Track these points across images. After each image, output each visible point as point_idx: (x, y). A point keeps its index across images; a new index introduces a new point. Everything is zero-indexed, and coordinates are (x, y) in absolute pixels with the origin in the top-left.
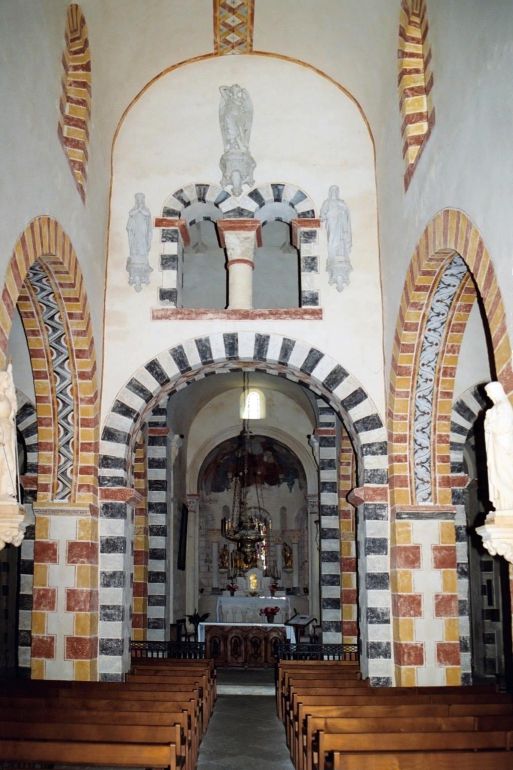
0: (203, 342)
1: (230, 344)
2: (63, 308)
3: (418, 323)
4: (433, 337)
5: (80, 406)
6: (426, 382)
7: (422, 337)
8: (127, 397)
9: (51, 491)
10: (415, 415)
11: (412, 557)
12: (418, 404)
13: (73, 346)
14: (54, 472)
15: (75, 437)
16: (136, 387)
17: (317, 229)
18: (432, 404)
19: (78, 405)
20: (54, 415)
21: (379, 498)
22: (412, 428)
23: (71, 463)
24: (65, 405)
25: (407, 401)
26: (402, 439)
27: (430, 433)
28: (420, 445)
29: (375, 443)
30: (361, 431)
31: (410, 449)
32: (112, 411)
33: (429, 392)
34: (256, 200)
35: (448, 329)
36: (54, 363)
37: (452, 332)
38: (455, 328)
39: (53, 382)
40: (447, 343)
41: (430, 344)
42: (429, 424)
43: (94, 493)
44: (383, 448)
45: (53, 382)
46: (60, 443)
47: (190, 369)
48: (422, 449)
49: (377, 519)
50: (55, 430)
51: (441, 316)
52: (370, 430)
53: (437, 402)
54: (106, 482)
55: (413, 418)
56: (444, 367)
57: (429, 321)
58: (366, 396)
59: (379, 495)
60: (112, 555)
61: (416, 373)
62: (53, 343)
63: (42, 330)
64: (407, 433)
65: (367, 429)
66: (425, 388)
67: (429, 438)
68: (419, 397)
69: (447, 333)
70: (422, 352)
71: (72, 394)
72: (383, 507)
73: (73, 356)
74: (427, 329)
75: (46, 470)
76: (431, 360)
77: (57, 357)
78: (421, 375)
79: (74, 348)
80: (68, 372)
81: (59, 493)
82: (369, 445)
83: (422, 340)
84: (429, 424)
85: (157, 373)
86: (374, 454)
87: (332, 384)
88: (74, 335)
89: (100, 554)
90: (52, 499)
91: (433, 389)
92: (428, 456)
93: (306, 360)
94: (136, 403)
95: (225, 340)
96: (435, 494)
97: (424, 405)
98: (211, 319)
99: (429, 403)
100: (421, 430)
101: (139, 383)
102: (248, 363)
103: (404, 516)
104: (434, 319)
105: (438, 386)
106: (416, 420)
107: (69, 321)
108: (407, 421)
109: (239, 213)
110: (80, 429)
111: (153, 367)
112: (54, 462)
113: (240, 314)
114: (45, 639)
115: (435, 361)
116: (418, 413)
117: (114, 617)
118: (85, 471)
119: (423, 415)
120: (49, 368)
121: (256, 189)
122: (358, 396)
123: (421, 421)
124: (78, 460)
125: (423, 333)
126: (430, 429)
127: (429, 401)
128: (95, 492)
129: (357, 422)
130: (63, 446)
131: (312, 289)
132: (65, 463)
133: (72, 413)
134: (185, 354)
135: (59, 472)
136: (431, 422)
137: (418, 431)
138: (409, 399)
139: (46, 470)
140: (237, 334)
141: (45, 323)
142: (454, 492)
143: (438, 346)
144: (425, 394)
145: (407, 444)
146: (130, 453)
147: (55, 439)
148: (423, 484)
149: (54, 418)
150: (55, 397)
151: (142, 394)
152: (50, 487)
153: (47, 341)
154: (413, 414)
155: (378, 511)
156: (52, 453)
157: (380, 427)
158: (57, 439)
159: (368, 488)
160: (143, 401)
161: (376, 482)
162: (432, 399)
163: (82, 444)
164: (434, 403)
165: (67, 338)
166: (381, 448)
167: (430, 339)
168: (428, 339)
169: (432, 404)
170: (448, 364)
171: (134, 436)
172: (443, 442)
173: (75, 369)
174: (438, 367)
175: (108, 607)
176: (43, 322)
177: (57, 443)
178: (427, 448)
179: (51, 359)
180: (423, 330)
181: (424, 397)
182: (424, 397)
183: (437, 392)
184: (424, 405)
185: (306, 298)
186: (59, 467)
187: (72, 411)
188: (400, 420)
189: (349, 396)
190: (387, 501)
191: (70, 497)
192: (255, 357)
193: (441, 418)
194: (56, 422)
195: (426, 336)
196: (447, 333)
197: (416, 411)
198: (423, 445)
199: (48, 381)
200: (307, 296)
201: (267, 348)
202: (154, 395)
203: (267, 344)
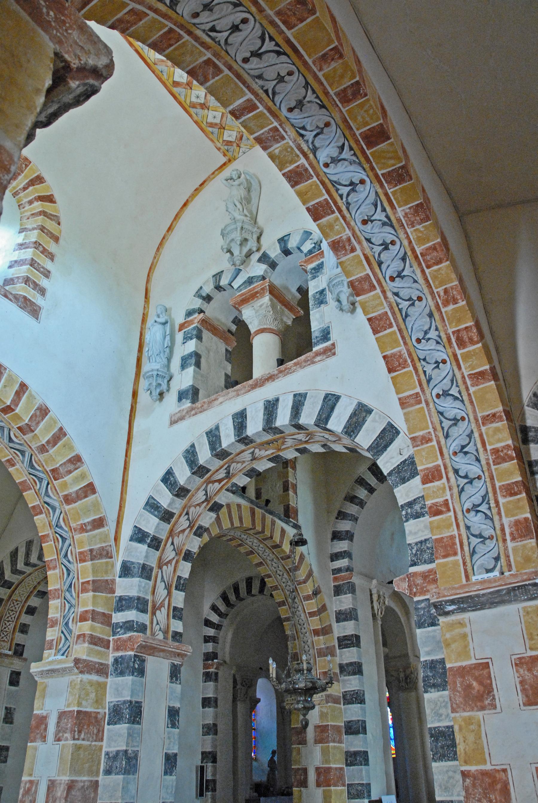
10: (443, 428)
12: (441, 409)
18: (462, 401)
22: (445, 450)
27: (477, 450)
28: (466, 477)
33: (450, 383)
48: (471, 482)
53: (469, 395)
64: (440, 462)
68: (438, 396)
92: (483, 492)
99: (457, 402)
100: (460, 452)
106: (447, 436)
108: (434, 443)
116: (446, 424)
119: (455, 424)
123: (456, 435)
127: (456, 398)
136: (472, 432)
137: (455, 453)
138: (423, 405)
144: (446, 388)
145: (444, 480)
162: (460, 392)
164: (466, 398)
169: (462, 401)
173: (58, 494)
178: (479, 478)
181: (446, 394)
182: (446, 394)
183: (463, 377)
188: (422, 444)
197: (441, 422)
198: (471, 476)
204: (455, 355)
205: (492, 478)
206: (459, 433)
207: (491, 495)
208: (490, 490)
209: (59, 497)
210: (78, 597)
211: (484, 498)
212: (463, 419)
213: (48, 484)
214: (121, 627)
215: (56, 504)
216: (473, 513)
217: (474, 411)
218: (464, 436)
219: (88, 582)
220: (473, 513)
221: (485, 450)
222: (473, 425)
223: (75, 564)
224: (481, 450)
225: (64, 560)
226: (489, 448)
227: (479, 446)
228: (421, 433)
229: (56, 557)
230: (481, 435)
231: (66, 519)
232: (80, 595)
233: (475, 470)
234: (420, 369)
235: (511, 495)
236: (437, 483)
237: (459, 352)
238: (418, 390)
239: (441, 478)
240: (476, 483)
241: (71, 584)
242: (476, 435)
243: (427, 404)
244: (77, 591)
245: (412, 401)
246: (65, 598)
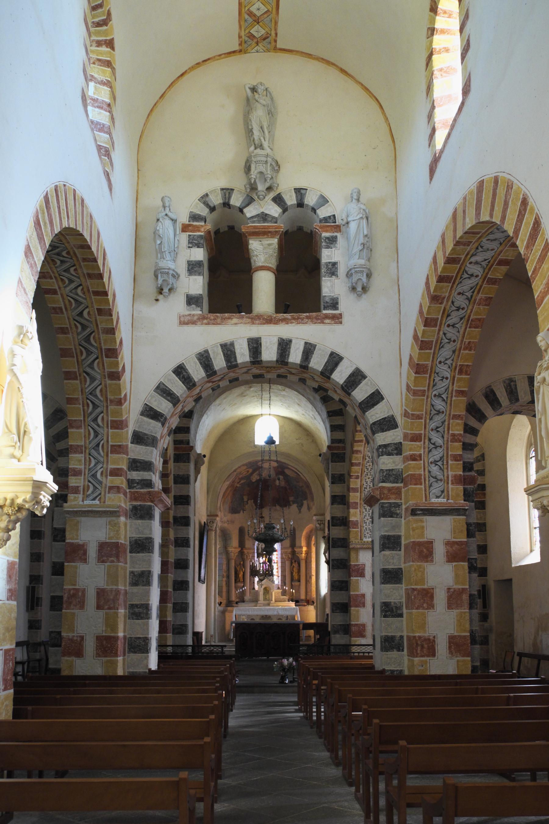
0: (228, 346)
1: (253, 348)
2: (92, 303)
3: (438, 318)
4: (451, 333)
5: (109, 407)
6: (442, 380)
7: (441, 333)
8: (155, 401)
9: (82, 492)
10: (430, 414)
11: (424, 551)
12: (433, 403)
13: (102, 344)
14: (85, 474)
15: (105, 439)
16: (163, 391)
17: (338, 235)
18: (446, 403)
19: (107, 407)
20: (84, 417)
21: (394, 496)
23: (101, 465)
24: (95, 406)
25: (424, 399)
26: (416, 438)
27: (444, 431)
28: (434, 444)
29: (391, 444)
30: (378, 433)
31: (424, 448)
32: (141, 415)
33: (444, 391)
34: (279, 205)
35: (467, 324)
36: (83, 363)
37: (470, 328)
38: (473, 323)
39: (83, 382)
40: (464, 340)
41: (447, 341)
42: (443, 423)
43: (124, 494)
44: (397, 449)
45: (83, 382)
46: (90, 446)
47: (215, 373)
48: (436, 448)
49: (391, 517)
50: (85, 432)
51: (461, 310)
52: (386, 431)
53: (451, 401)
54: (136, 485)
55: (428, 417)
56: (460, 365)
57: (448, 315)
58: (383, 398)
59: (394, 493)
60: (141, 554)
61: (433, 371)
62: (83, 342)
63: (71, 328)
64: (423, 432)
65: (383, 430)
66: (442, 386)
67: (443, 437)
68: (435, 396)
69: (466, 328)
70: (439, 349)
71: (102, 395)
72: (398, 506)
73: (102, 354)
74: (446, 324)
75: (77, 473)
76: (448, 357)
77: (87, 357)
78: (437, 373)
79: (103, 347)
80: (97, 372)
81: (89, 495)
82: (385, 446)
83: (441, 336)
84: (443, 423)
85: (183, 377)
86: (389, 454)
87: (351, 387)
88: (103, 333)
89: (129, 554)
90: (83, 501)
91: (448, 387)
92: (441, 455)
93: (326, 363)
94: (163, 406)
95: (249, 345)
96: (448, 491)
97: (439, 404)
98: (236, 324)
99: (444, 402)
100: (435, 429)
101: (167, 387)
102: (271, 367)
103: (419, 512)
104: (454, 314)
105: (453, 384)
106: (431, 419)
107: (98, 317)
108: (423, 421)
109: (263, 218)
110: (110, 431)
111: (180, 371)
112: (85, 464)
113: (263, 319)
114: (75, 638)
115: (452, 358)
117: (142, 615)
118: (116, 473)
119: (438, 414)
120: (79, 368)
121: (279, 194)
122: (376, 398)
123: (436, 420)
124: (108, 462)
125: (442, 329)
126: (444, 428)
127: (444, 400)
128: (125, 494)
129: (374, 424)
130: (93, 448)
131: (332, 295)
132: (95, 465)
133: (102, 415)
134: (211, 359)
135: (89, 475)
136: (445, 421)
137: (432, 430)
138: (425, 398)
139: (77, 473)
140: (261, 338)
141: (74, 320)
142: (465, 490)
143: (456, 343)
144: (441, 393)
146: (158, 458)
147: (85, 442)
148: (436, 482)
149: (84, 420)
150: (85, 399)
151: (169, 398)
152: (81, 489)
153: (77, 340)
154: (428, 413)
155: (393, 509)
156: (83, 455)
157: (395, 428)
158: (87, 442)
159: (384, 487)
160: (170, 405)
161: (390, 482)
162: (447, 398)
163: (112, 446)
164: (449, 402)
165: (97, 336)
166: (396, 449)
167: (449, 335)
168: (447, 335)
169: (446, 403)
170: (463, 362)
171: (162, 441)
172: (456, 441)
173: (104, 369)
174: (454, 365)
175: (137, 606)
176: (72, 319)
177: (87, 446)
178: (441, 447)
179: (80, 359)
180: (442, 326)
181: (440, 396)
182: (440, 396)
183: (452, 390)
184: (439, 404)
185: (327, 302)
186: (89, 469)
187: (102, 412)
188: (416, 419)
189: (367, 398)
190: (401, 499)
191: (100, 498)
192: (277, 361)
193: (456, 417)
194: (86, 424)
195: (446, 332)
196: (466, 328)
197: (431, 410)
198: (437, 444)
199: (78, 382)
200: (328, 301)
201: (289, 352)
202: (181, 399)
203: (290, 348)
204: (454, 377)
205: (447, 449)
206: (438, 419)
207: (445, 457)
208: (445, 455)
209: (104, 372)
210: (107, 456)
211: (441, 458)
212: (443, 412)
213: (97, 358)
214: (138, 483)
215: (98, 377)
216: (434, 465)
217: (450, 410)
218: (440, 422)
219: (120, 446)
220: (434, 465)
221: (448, 432)
222: (447, 418)
223: (105, 429)
224: (446, 432)
225: (92, 423)
226: (451, 432)
227: (446, 429)
228: (418, 413)
229: (82, 419)
230: (449, 424)
231: (104, 391)
232: (110, 455)
233: (439, 441)
234: (432, 377)
235: (456, 460)
236: (418, 443)
237: (457, 376)
238: (426, 389)
239: (421, 441)
240: (438, 449)
241: (99, 444)
242: (446, 423)
243: (427, 398)
244: (105, 451)
245: (420, 393)
246: (90, 454)
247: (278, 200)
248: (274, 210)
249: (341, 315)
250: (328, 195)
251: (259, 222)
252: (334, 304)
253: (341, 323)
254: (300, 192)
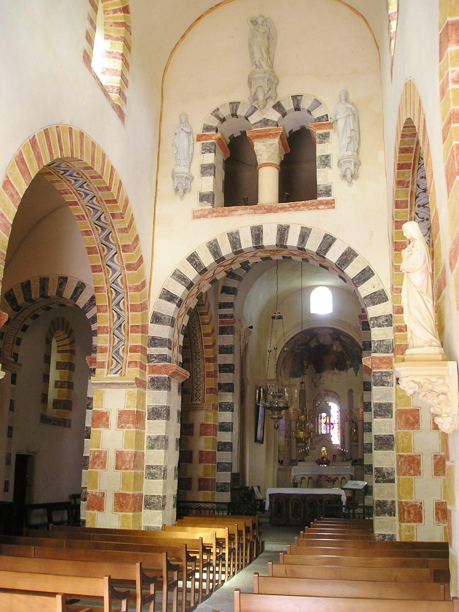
247: (278, 107)
248: (275, 116)
249: (333, 200)
250: (320, 98)
251: (261, 127)
252: (328, 192)
253: (334, 208)
254: (296, 99)
